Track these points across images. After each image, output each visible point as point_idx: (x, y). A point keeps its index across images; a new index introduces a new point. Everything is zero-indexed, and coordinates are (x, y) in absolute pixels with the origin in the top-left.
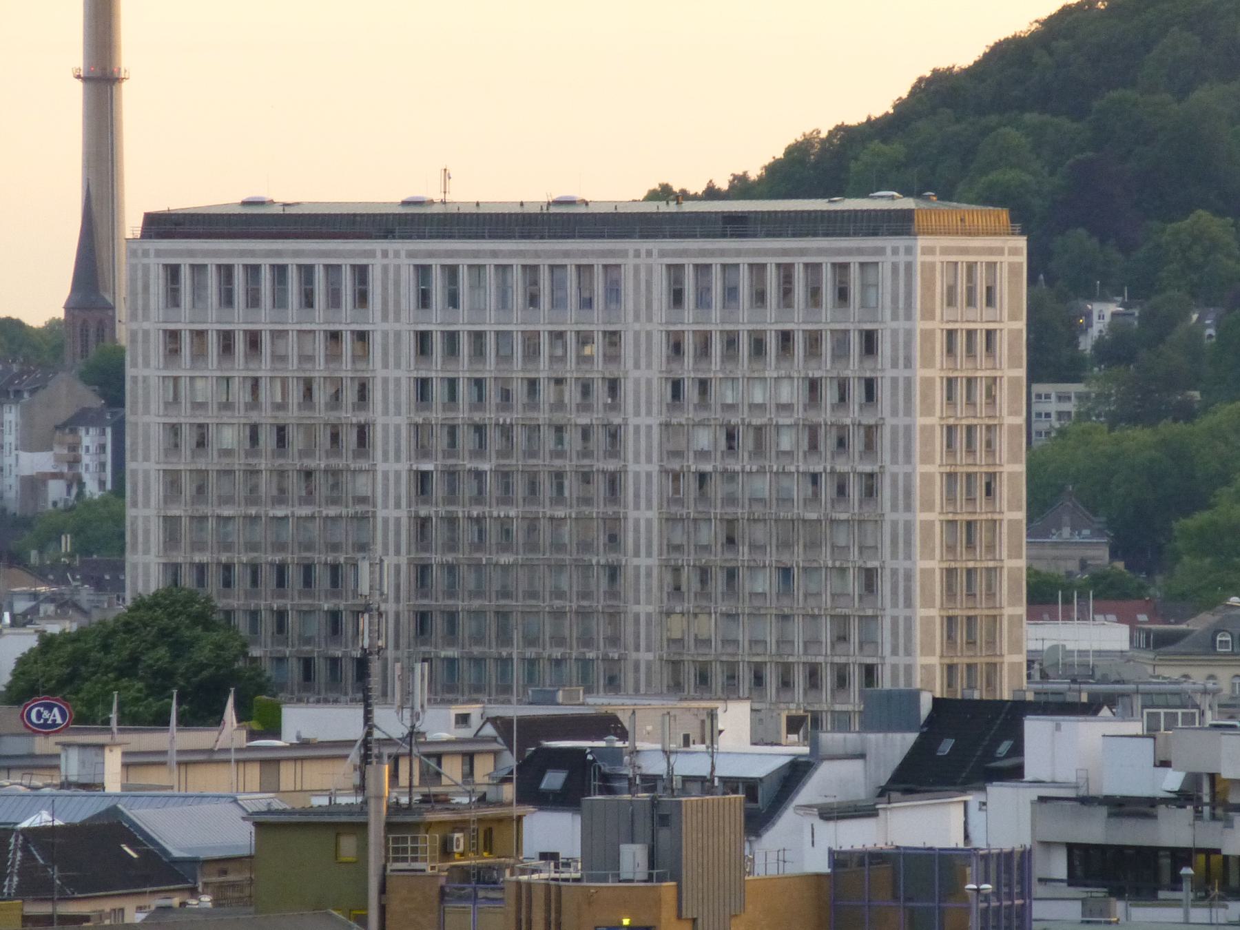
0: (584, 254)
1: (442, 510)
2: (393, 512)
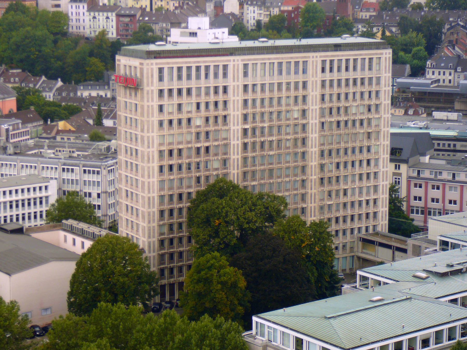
0: (297, 58)
1: (252, 140)
2: (236, 142)
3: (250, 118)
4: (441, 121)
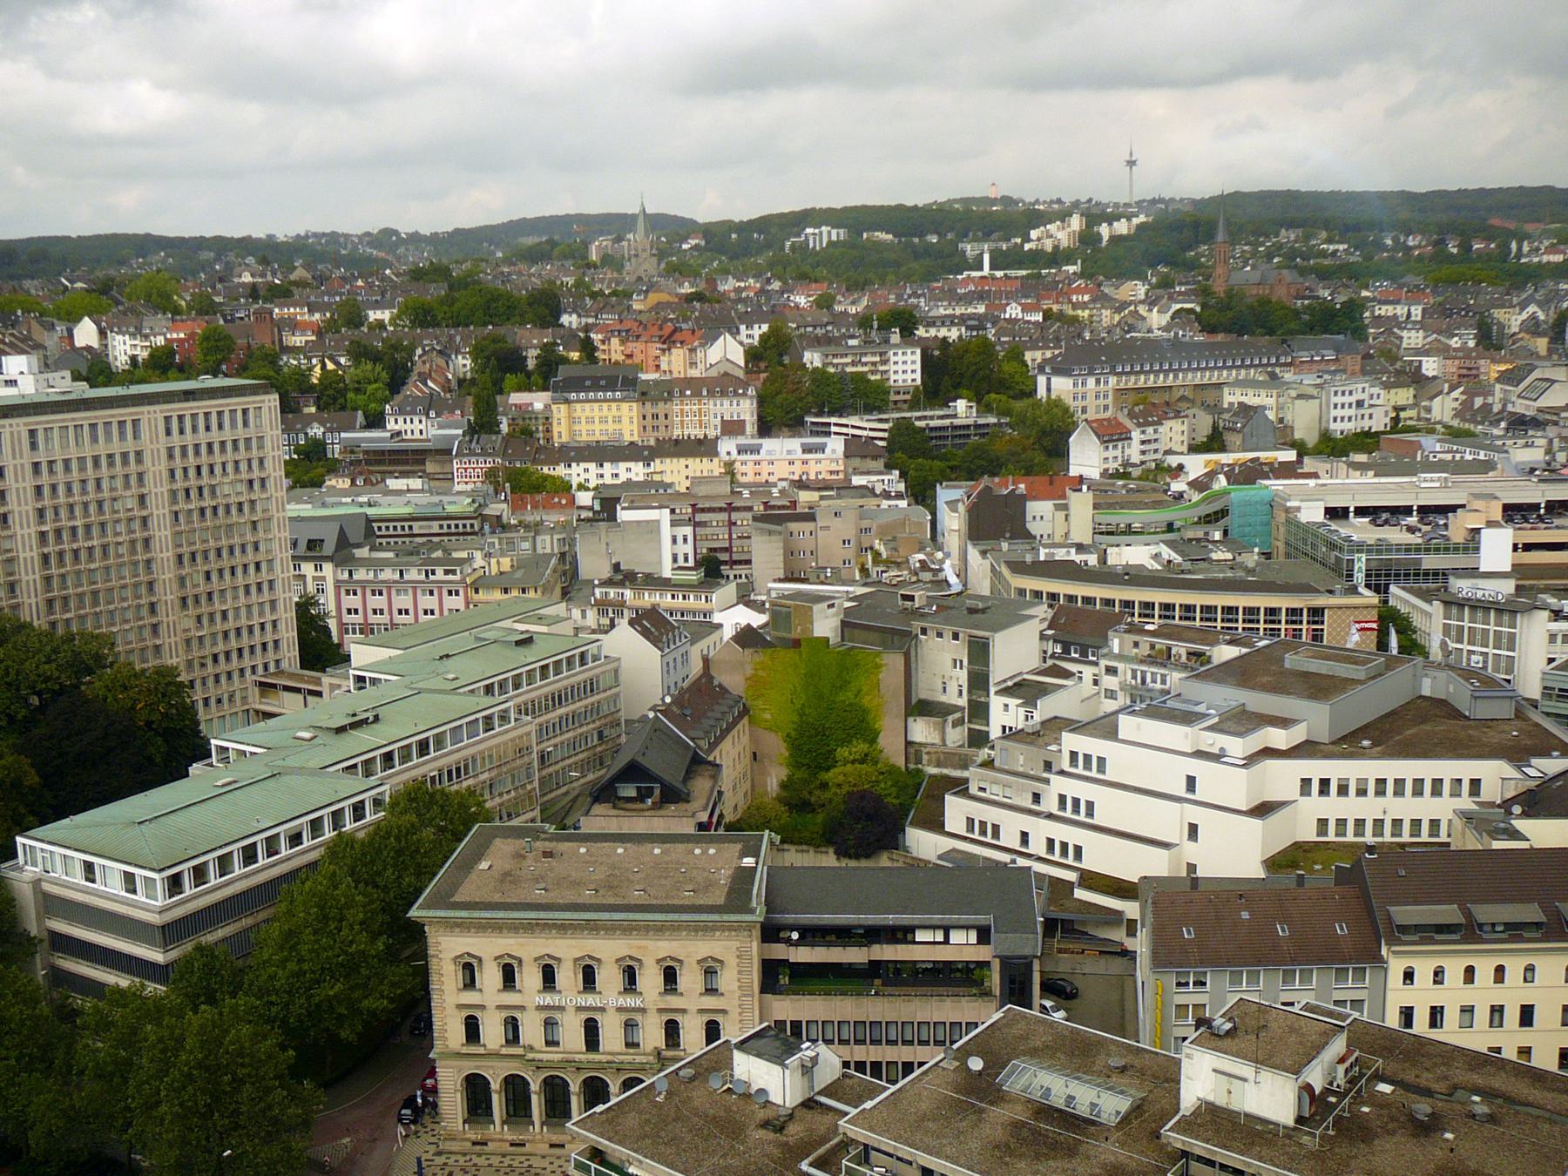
1: (57, 548)
2: (28, 554)
3: (49, 514)
4: (399, 493)
